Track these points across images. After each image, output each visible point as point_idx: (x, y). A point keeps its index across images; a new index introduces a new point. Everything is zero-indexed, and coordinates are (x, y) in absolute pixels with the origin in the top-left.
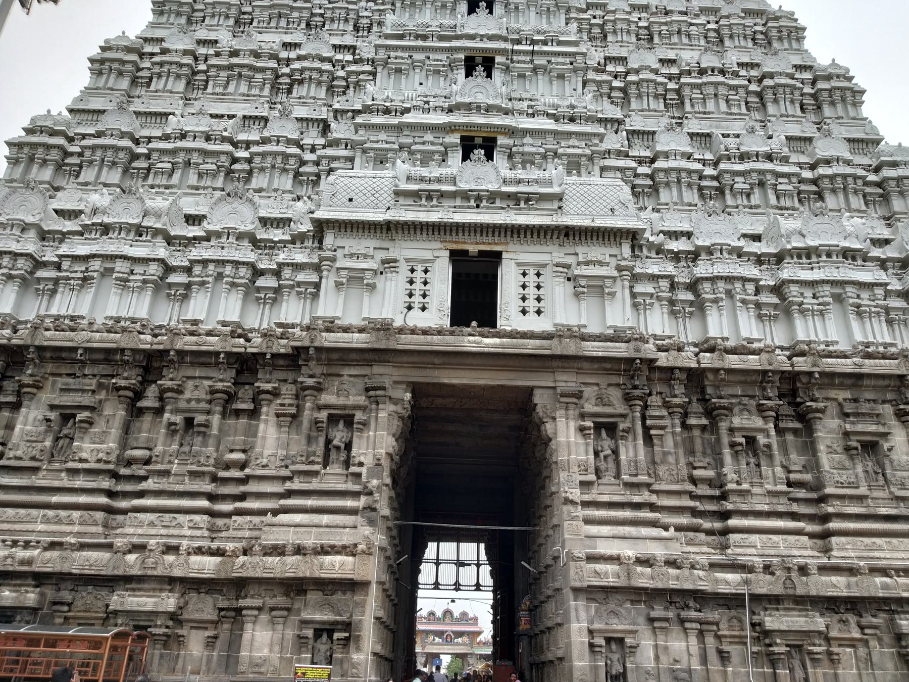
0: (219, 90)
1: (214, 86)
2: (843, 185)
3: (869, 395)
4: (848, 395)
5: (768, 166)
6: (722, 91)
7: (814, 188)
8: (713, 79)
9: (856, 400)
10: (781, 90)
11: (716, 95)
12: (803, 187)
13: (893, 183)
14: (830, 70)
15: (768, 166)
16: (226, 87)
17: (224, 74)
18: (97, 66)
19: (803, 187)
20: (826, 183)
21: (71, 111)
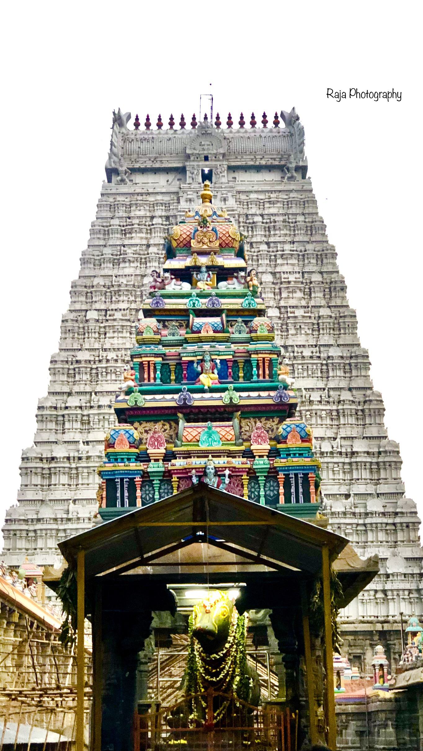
0: (86, 481)
1: (82, 479)
2: (375, 527)
3: (361, 637)
4: (353, 638)
5: (343, 521)
6: (331, 465)
7: (364, 528)
8: (326, 460)
9: (355, 640)
10: (359, 464)
11: (327, 467)
12: (359, 528)
13: (399, 525)
14: (387, 449)
15: (343, 521)
16: (88, 478)
17: (85, 470)
18: (24, 471)
19: (359, 528)
20: (369, 527)
21: (19, 501)
